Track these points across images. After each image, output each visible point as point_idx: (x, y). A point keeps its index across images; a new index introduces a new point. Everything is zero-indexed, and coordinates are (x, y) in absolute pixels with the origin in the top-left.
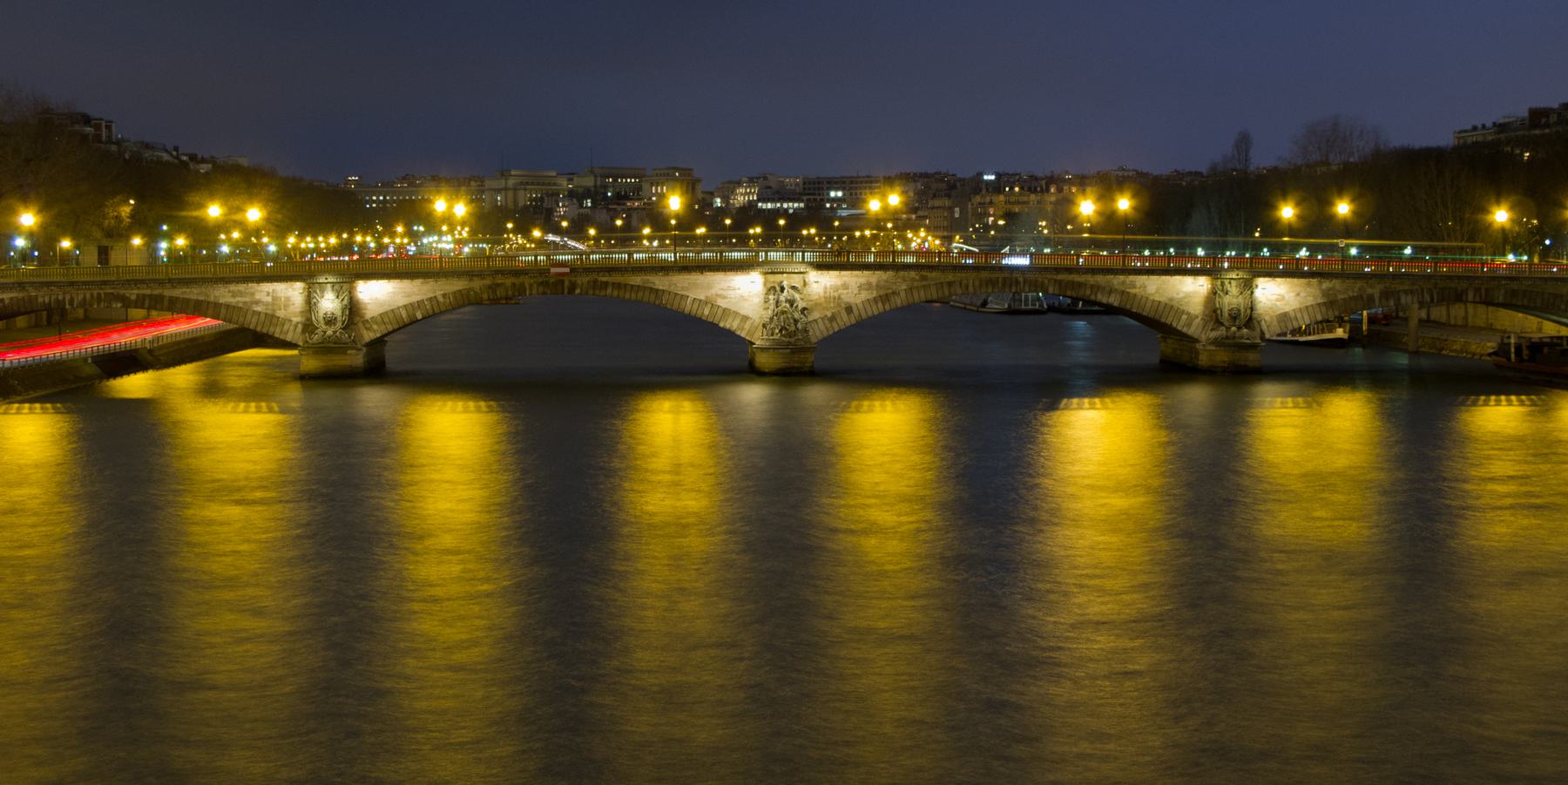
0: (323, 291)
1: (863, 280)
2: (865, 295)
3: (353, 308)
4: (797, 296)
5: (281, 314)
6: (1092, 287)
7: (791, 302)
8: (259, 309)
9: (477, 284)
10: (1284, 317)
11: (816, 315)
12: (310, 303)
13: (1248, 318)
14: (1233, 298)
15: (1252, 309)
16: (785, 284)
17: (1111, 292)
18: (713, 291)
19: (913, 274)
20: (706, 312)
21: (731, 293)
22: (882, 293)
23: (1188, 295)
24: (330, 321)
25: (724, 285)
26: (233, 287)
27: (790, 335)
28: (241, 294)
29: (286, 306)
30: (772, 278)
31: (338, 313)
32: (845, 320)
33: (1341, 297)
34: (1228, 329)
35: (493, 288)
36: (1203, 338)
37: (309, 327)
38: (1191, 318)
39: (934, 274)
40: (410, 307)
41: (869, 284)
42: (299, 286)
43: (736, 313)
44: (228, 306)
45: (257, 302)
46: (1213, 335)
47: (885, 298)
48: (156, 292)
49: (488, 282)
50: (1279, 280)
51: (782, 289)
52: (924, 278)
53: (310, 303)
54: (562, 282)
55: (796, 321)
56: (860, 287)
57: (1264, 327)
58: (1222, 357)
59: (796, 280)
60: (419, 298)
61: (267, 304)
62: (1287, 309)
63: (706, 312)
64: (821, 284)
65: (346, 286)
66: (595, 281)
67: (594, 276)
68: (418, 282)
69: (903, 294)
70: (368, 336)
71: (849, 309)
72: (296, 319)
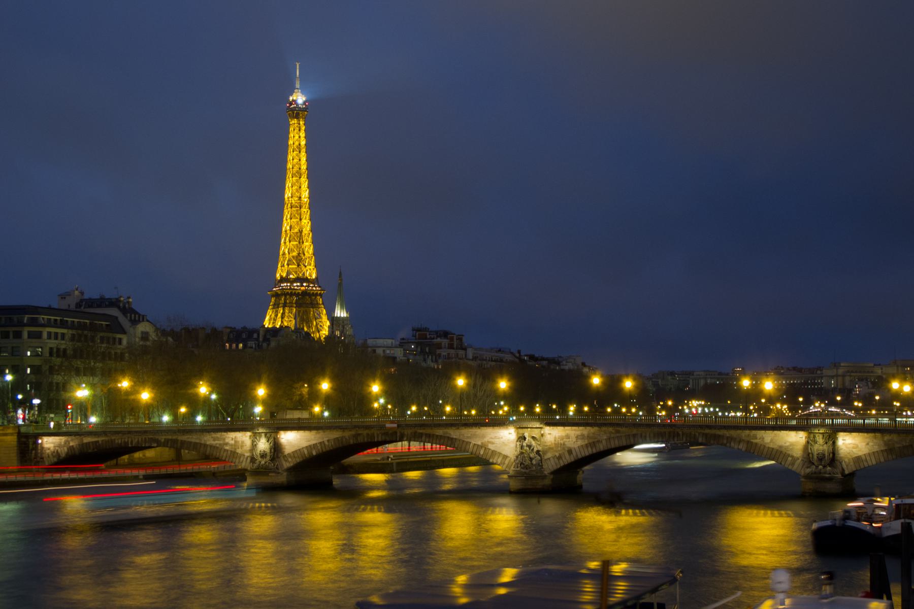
0: (260, 437)
1: (579, 433)
2: (580, 443)
3: (277, 447)
4: (533, 443)
5: (239, 451)
6: (728, 438)
7: (529, 446)
8: (227, 448)
9: (347, 434)
10: (858, 459)
11: (549, 455)
14: (820, 446)
15: (834, 453)
16: (526, 435)
17: (740, 442)
18: (486, 440)
19: (611, 429)
20: (482, 453)
21: (496, 441)
22: (591, 441)
23: (792, 444)
24: (263, 455)
25: (492, 435)
26: (214, 435)
27: (526, 467)
28: (218, 439)
29: (242, 446)
30: (521, 431)
31: (268, 451)
32: (568, 459)
33: (897, 446)
34: (817, 467)
35: (357, 436)
36: (802, 473)
37: (253, 459)
38: (795, 459)
39: (624, 429)
40: (309, 448)
41: (583, 435)
42: (249, 434)
43: (500, 454)
44: (211, 446)
45: (227, 444)
46: (808, 470)
47: (592, 444)
48: (174, 437)
49: (353, 432)
50: (854, 434)
51: (525, 438)
52: (618, 432)
53: (254, 446)
54: (396, 433)
55: (531, 459)
56: (577, 437)
57: (845, 466)
58: (809, 486)
60: (314, 442)
61: (232, 445)
62: (860, 454)
63: (482, 453)
64: (552, 435)
65: (273, 435)
66: (415, 433)
68: (314, 432)
69: (604, 442)
70: (286, 465)
71: (570, 451)
72: (247, 454)
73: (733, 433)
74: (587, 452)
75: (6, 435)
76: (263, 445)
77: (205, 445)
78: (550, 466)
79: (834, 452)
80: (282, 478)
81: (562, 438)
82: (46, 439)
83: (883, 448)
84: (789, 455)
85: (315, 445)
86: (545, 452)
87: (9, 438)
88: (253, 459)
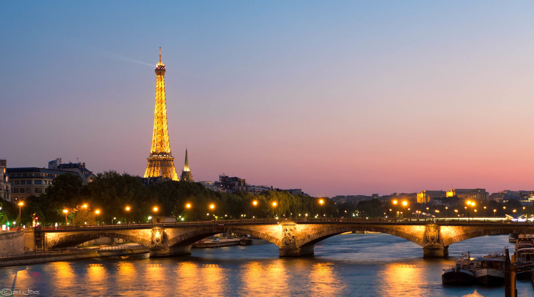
1: (313, 227)
2: (314, 232)
4: (291, 232)
7: (289, 234)
11: (299, 238)
12: (153, 236)
13: (439, 239)
14: (432, 232)
15: (439, 237)
16: (287, 228)
18: (268, 231)
19: (329, 225)
23: (418, 232)
24: (158, 241)
30: (284, 226)
32: (308, 240)
33: (470, 232)
37: (153, 243)
41: (315, 228)
42: (150, 230)
46: (426, 245)
47: (320, 233)
50: (449, 227)
52: (332, 226)
53: (153, 236)
55: (290, 240)
59: (292, 227)
64: (300, 228)
66: (233, 228)
67: (232, 226)
70: (169, 245)
71: (309, 236)
72: (150, 240)
73: (389, 226)
74: (317, 237)
75: (29, 232)
76: (158, 235)
77: (129, 236)
78: (298, 245)
79: (439, 235)
80: (167, 251)
81: (305, 230)
82: (48, 234)
83: (463, 233)
84: (417, 237)
85: (183, 235)
86: (297, 237)
87: (30, 234)
88: (153, 243)
